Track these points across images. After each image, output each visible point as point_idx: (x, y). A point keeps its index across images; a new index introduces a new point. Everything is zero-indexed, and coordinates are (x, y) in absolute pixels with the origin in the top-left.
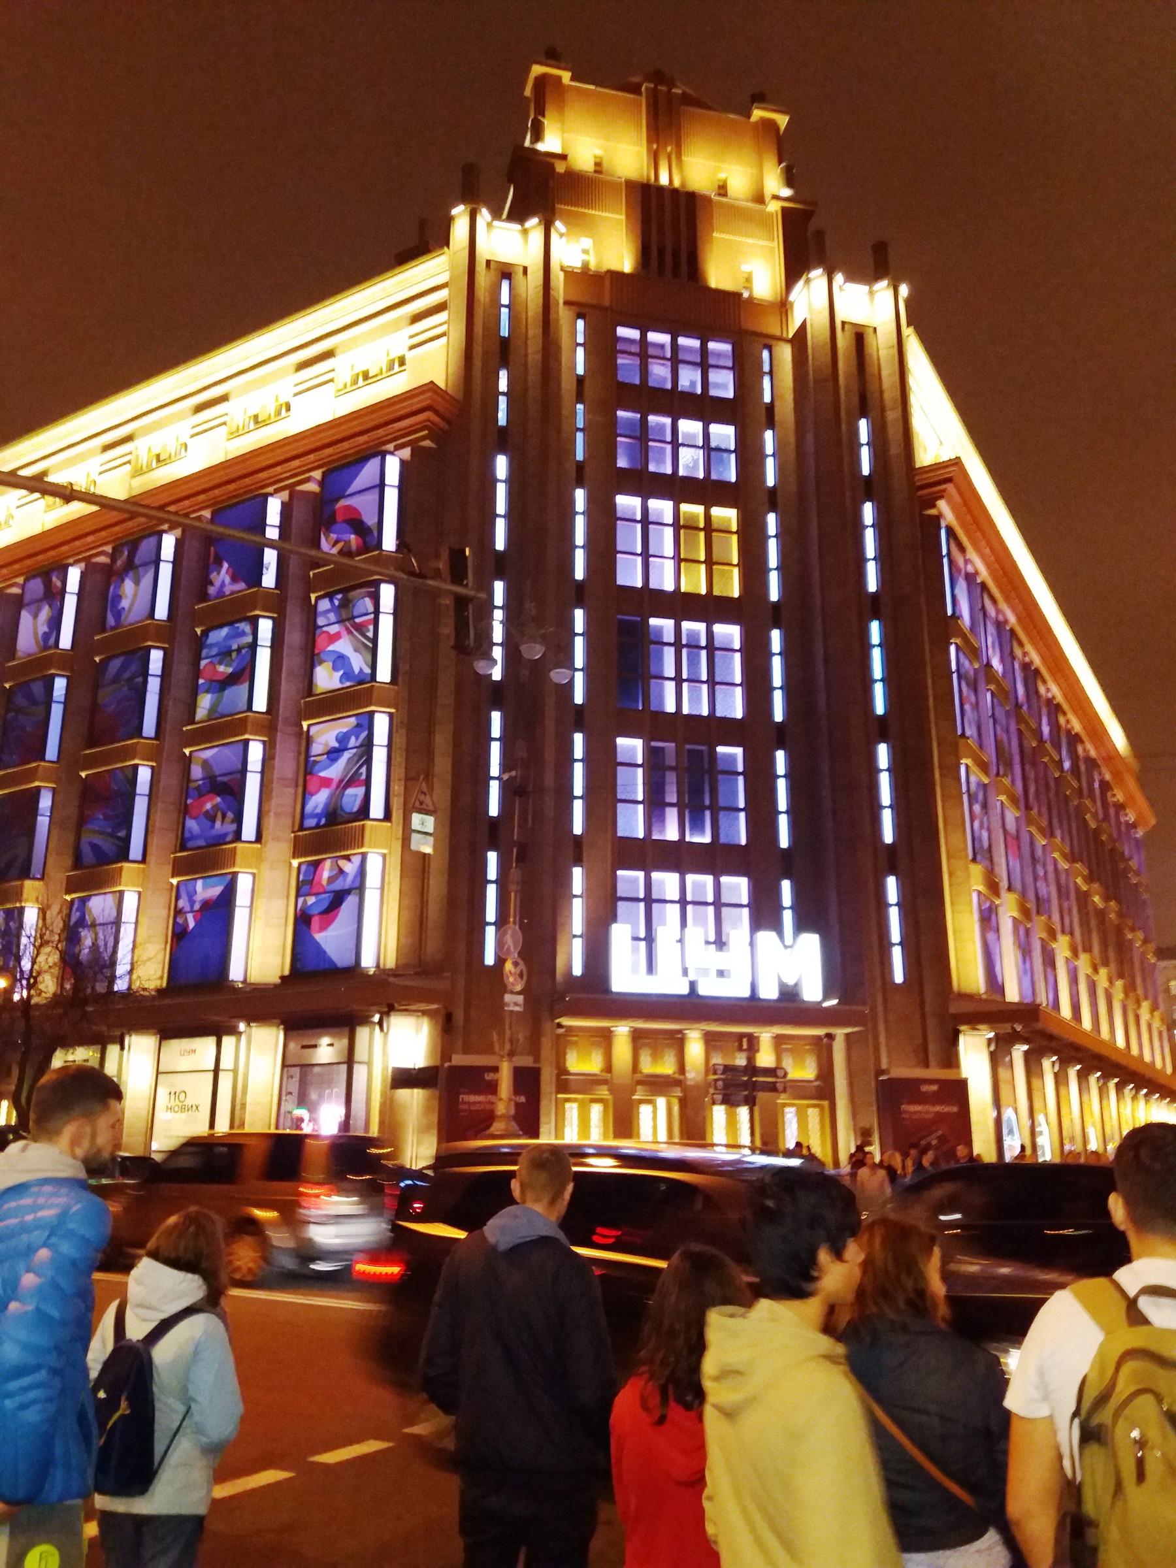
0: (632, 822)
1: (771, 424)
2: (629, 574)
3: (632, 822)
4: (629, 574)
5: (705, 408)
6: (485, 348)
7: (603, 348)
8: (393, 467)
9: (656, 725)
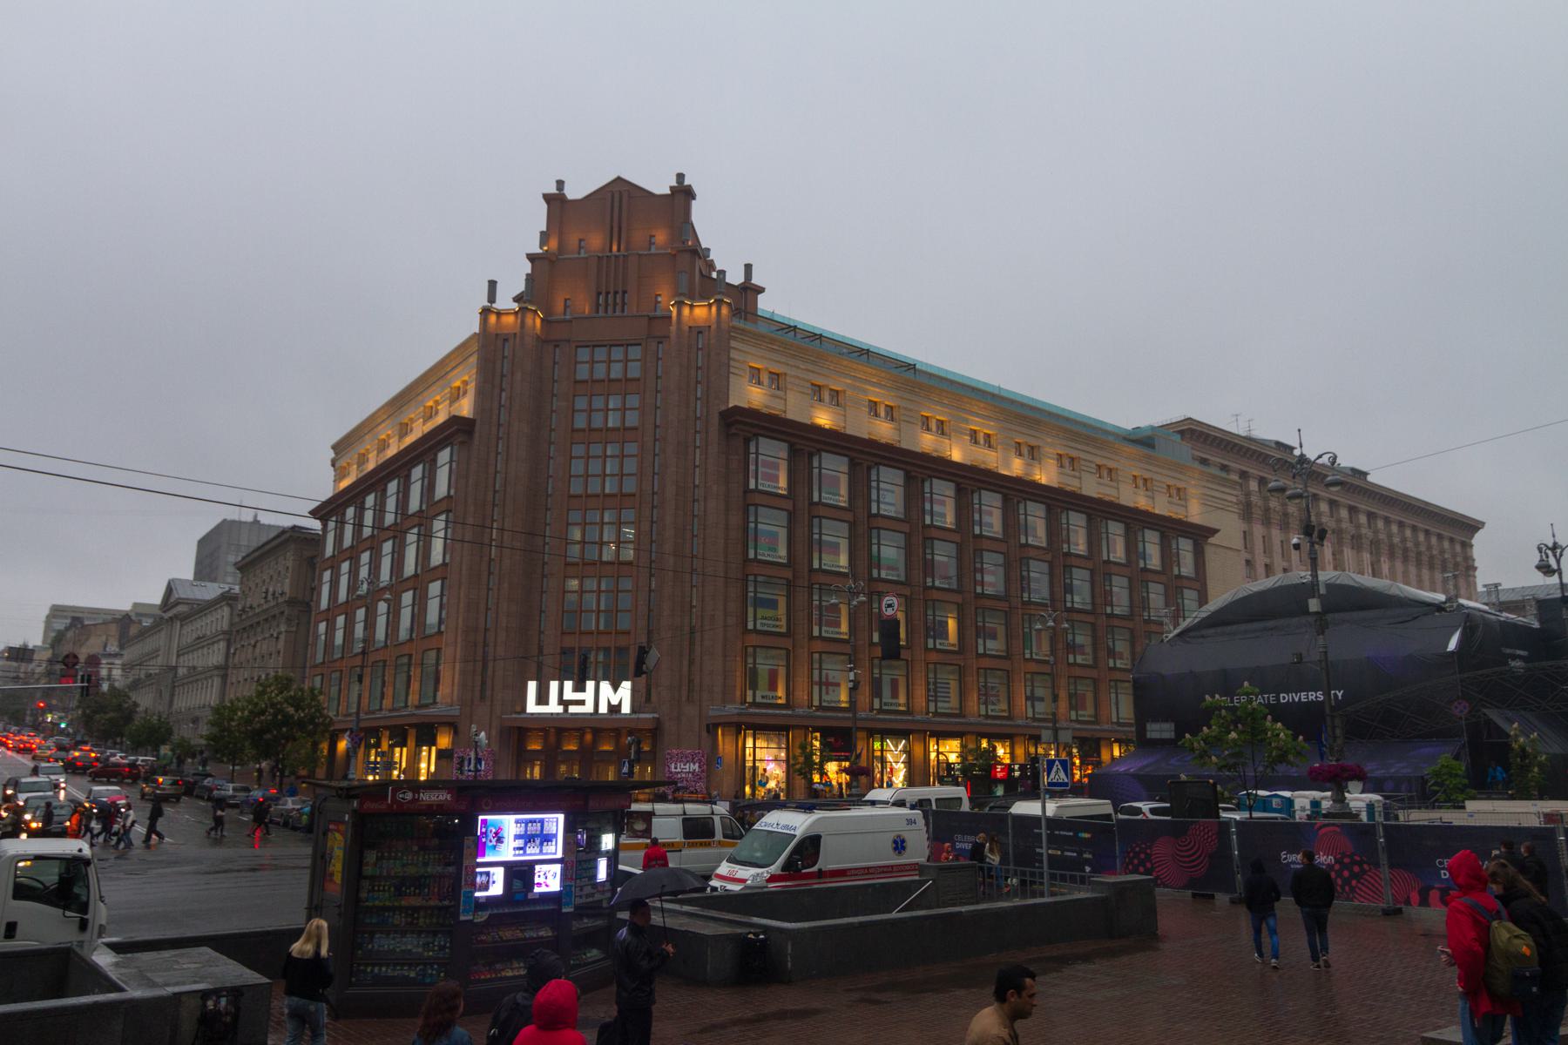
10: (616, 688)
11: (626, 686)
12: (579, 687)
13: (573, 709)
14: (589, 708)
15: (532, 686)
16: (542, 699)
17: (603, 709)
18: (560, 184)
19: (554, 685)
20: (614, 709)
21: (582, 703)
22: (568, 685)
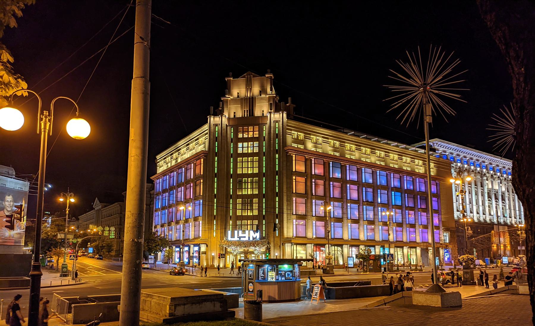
0: (239, 213)
1: (264, 140)
2: (239, 171)
3: (239, 213)
4: (239, 171)
5: (253, 139)
6: (213, 139)
7: (236, 133)
8: (202, 160)
9: (243, 197)
12: (244, 232)
13: (242, 239)
14: (247, 239)
16: (233, 236)
17: (251, 239)
19: (236, 232)
21: (245, 237)
22: (240, 232)
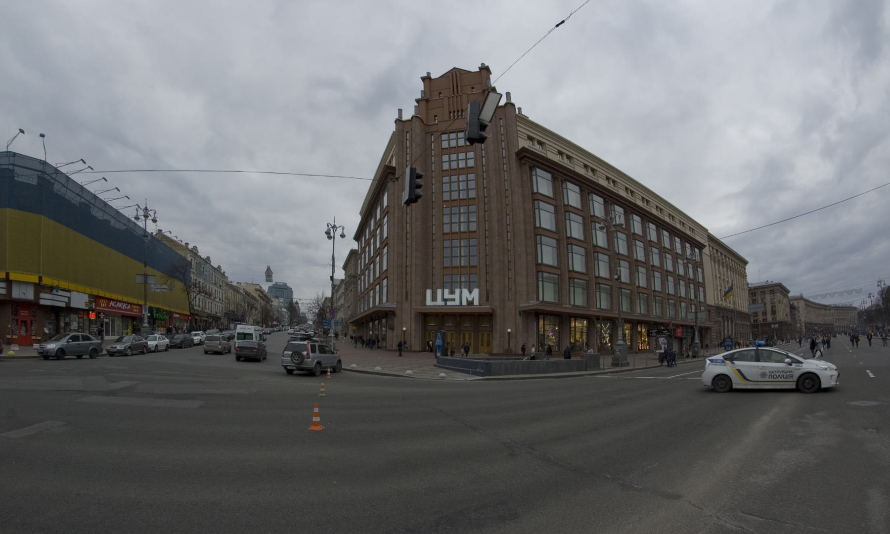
10: (470, 292)
11: (476, 292)
12: (452, 292)
13: (449, 303)
14: (457, 303)
15: (429, 293)
16: (434, 298)
17: (464, 303)
18: (400, 111)
19: (439, 292)
20: (470, 303)
21: (454, 300)
22: (446, 291)
